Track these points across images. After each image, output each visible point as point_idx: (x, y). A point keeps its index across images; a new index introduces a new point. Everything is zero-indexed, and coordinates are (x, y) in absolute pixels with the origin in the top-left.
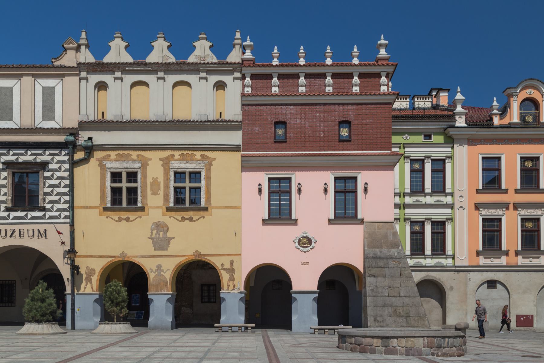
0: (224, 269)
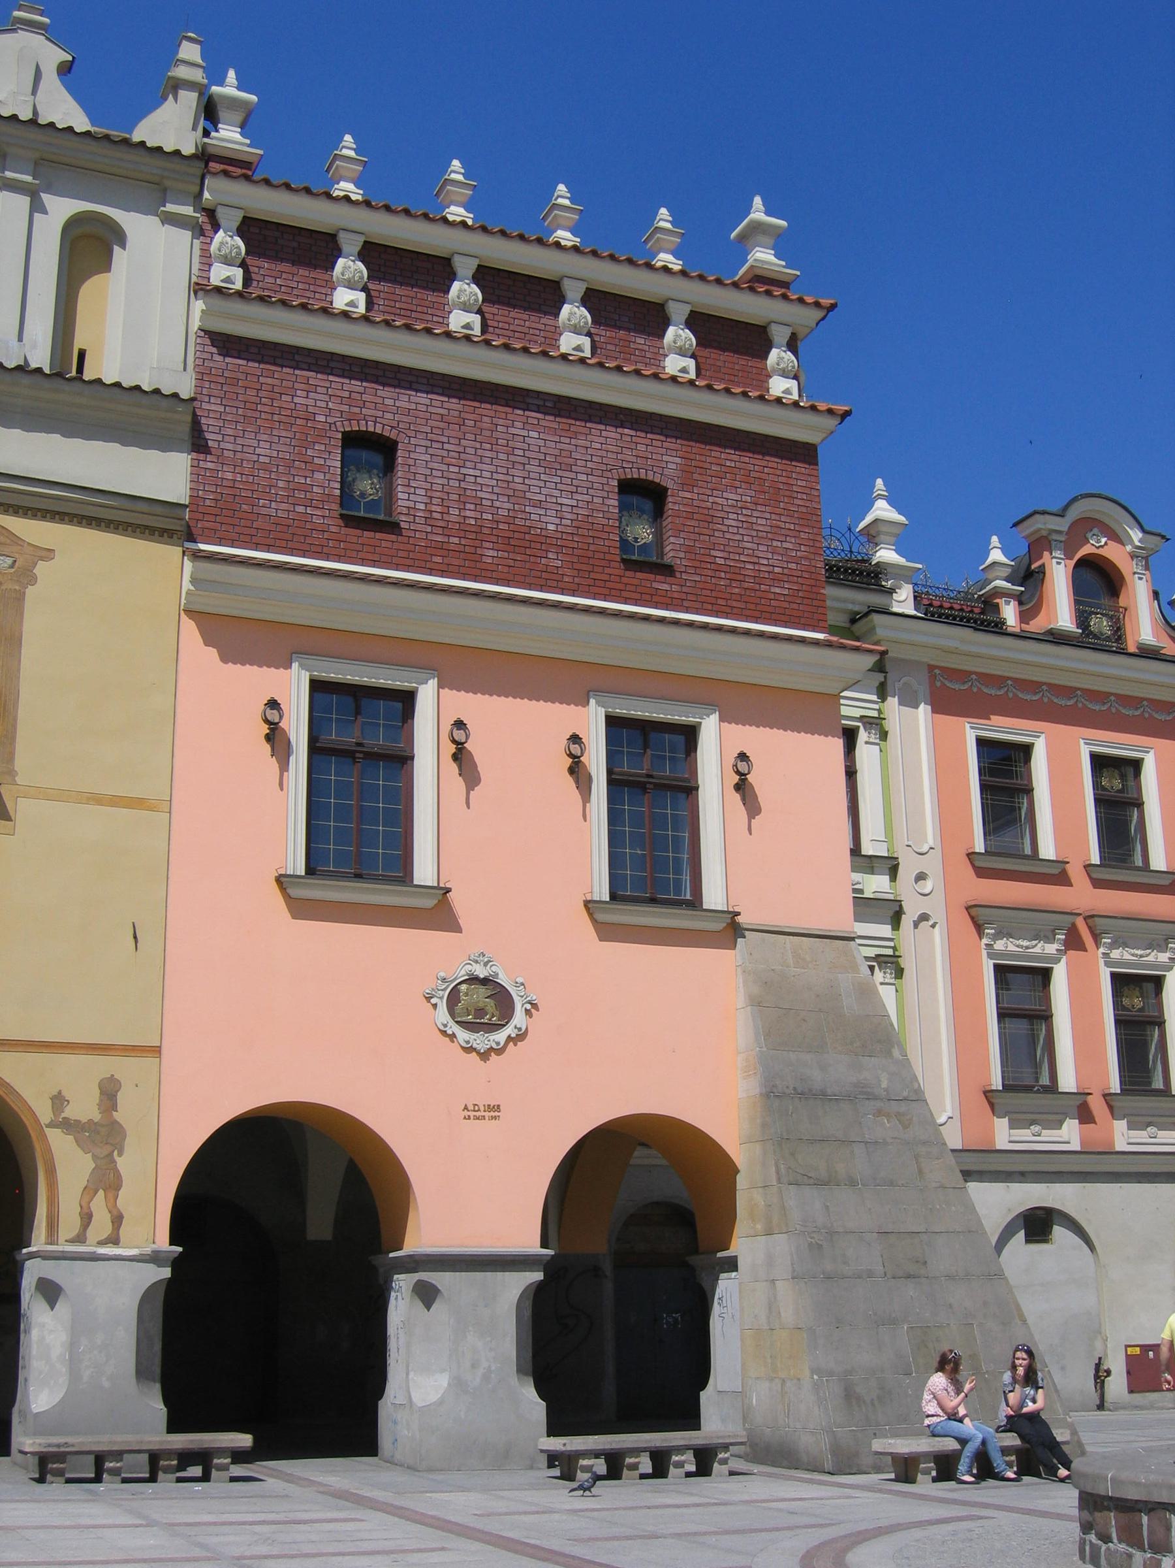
0: (67, 1125)
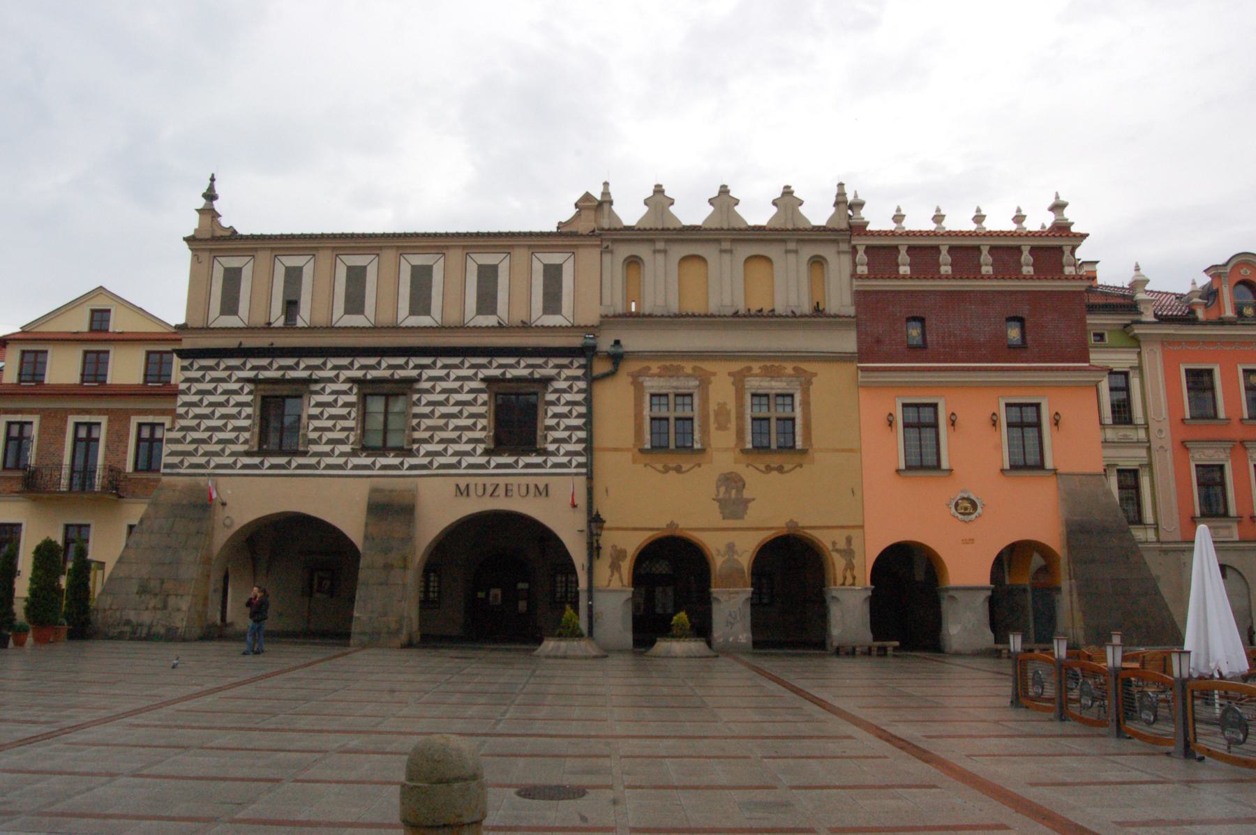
0: (837, 551)
